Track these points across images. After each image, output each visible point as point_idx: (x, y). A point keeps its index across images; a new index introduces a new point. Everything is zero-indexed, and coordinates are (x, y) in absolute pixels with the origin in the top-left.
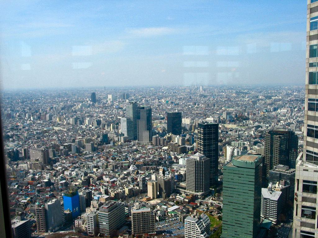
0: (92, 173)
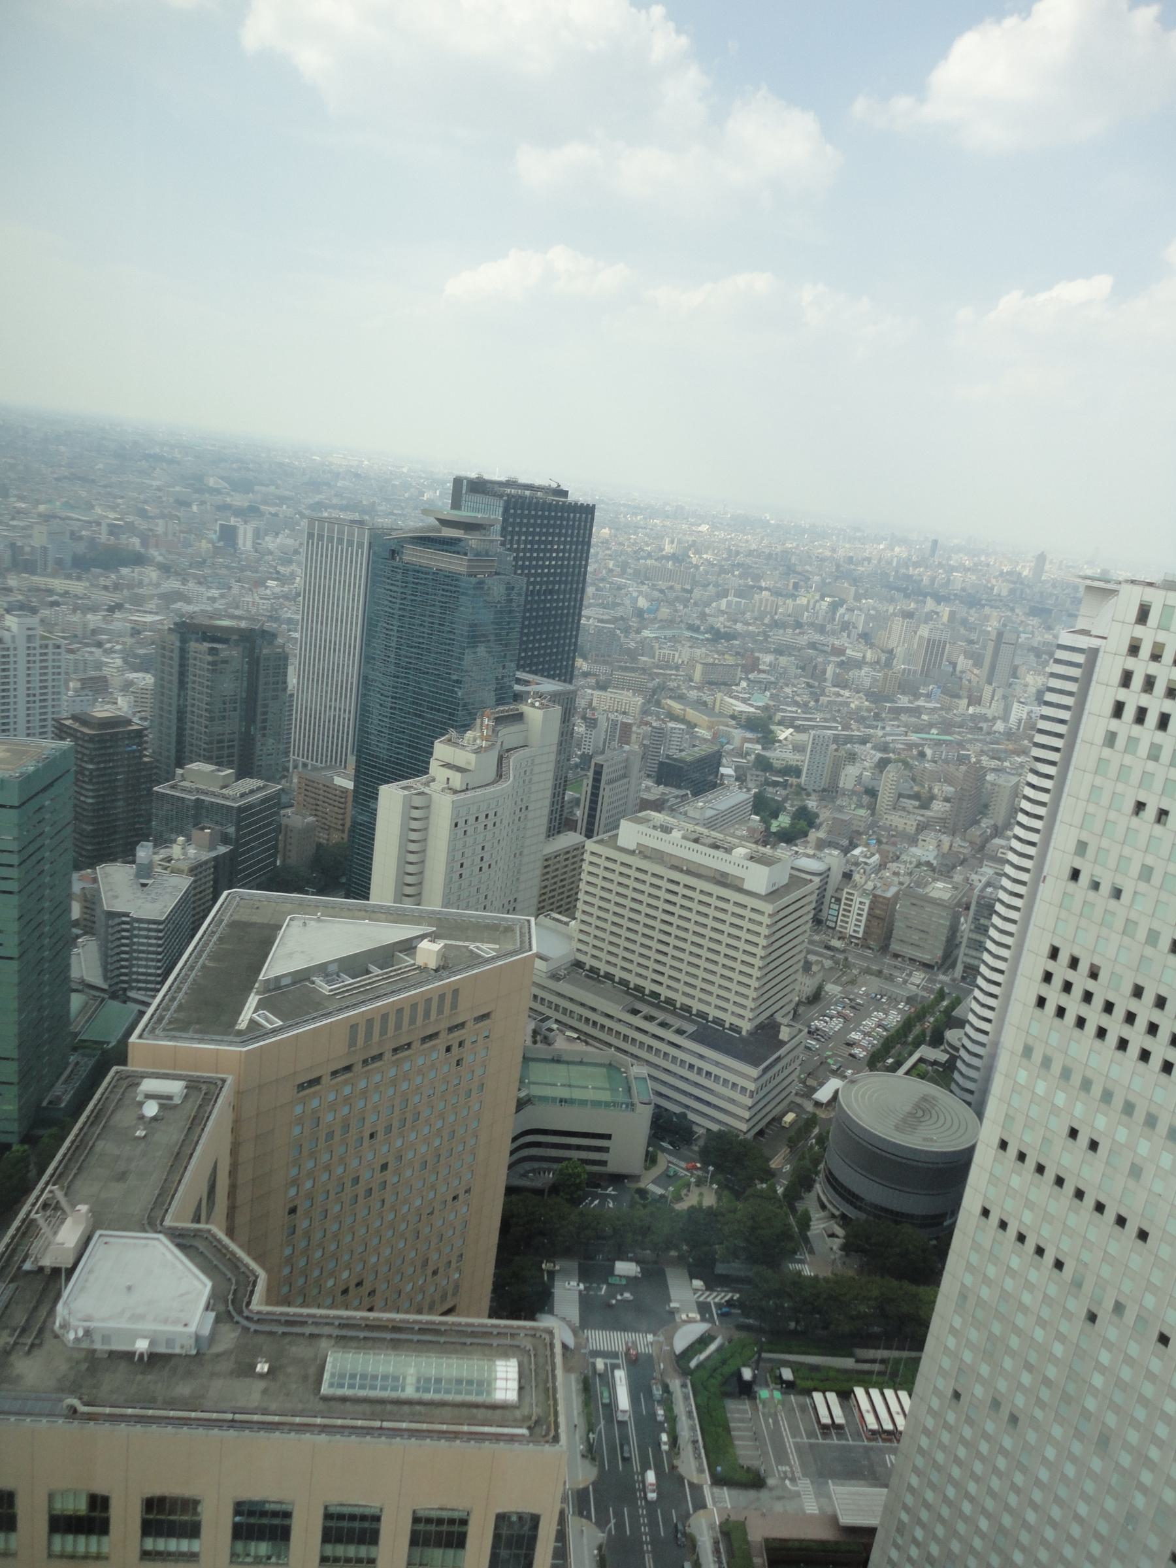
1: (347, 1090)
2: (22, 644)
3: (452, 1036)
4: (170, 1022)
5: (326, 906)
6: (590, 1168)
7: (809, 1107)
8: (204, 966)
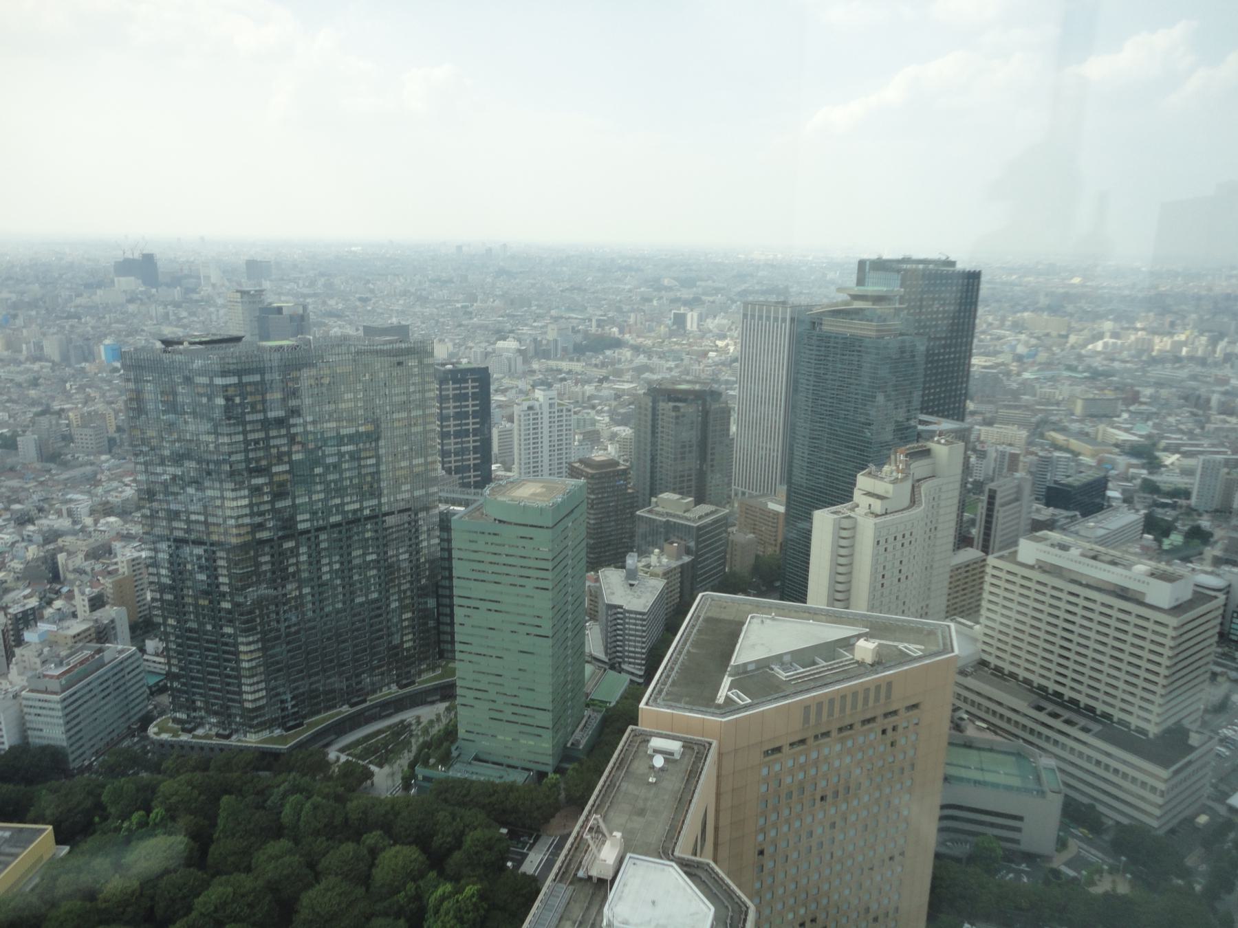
0: (75, 533)
1: (802, 759)
2: (546, 409)
3: (886, 721)
4: (667, 694)
5: (777, 607)
6: (1003, 844)
7: (1222, 810)
8: (688, 652)
